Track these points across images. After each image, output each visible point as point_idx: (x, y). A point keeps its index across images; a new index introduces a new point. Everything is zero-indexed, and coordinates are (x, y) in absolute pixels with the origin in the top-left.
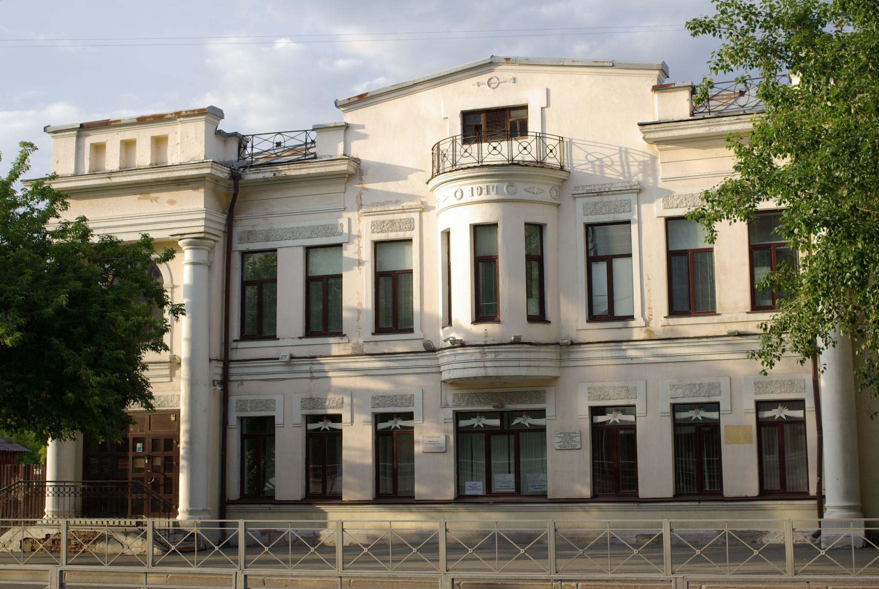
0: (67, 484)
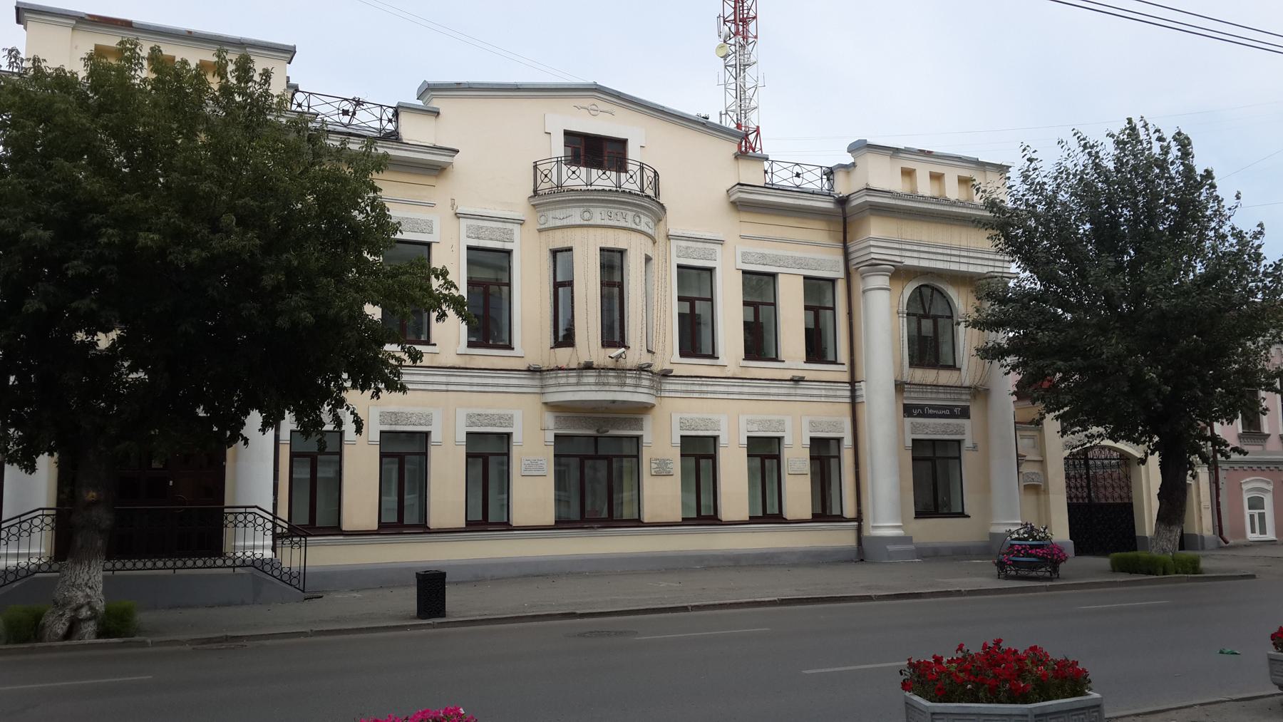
0: (23, 518)
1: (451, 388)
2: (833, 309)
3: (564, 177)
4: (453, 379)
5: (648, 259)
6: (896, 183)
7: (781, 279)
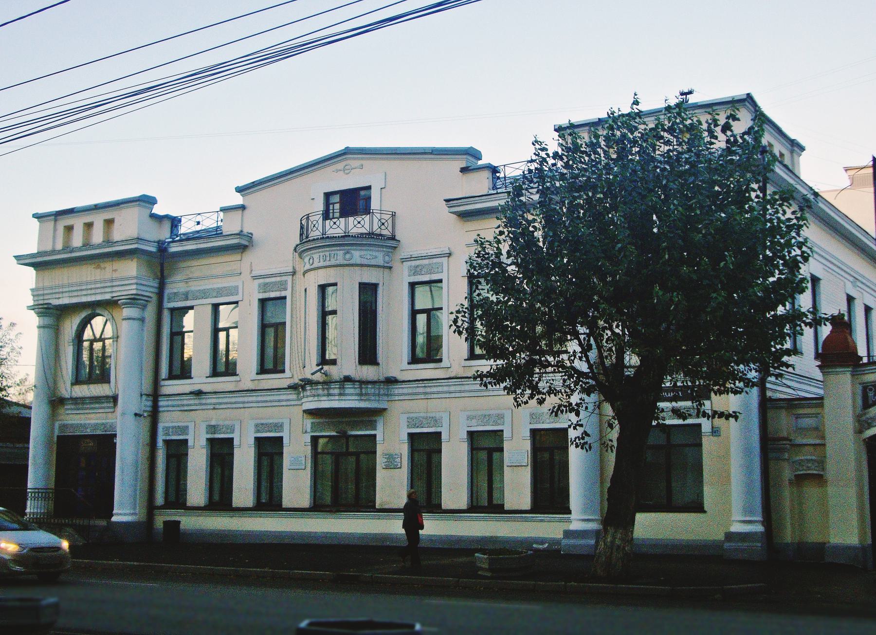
1: (246, 405)
4: (246, 399)
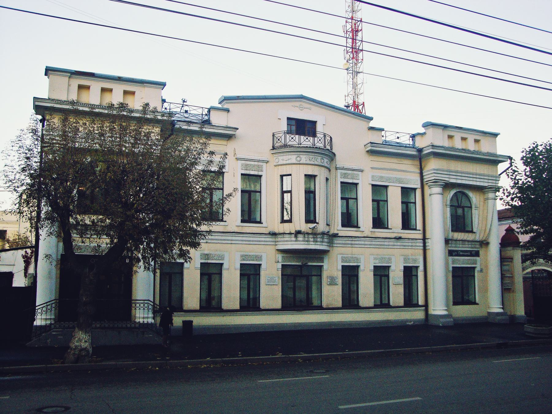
2: (415, 203)
3: (288, 140)
4: (234, 238)
5: (327, 179)
6: (446, 143)
7: (390, 189)
